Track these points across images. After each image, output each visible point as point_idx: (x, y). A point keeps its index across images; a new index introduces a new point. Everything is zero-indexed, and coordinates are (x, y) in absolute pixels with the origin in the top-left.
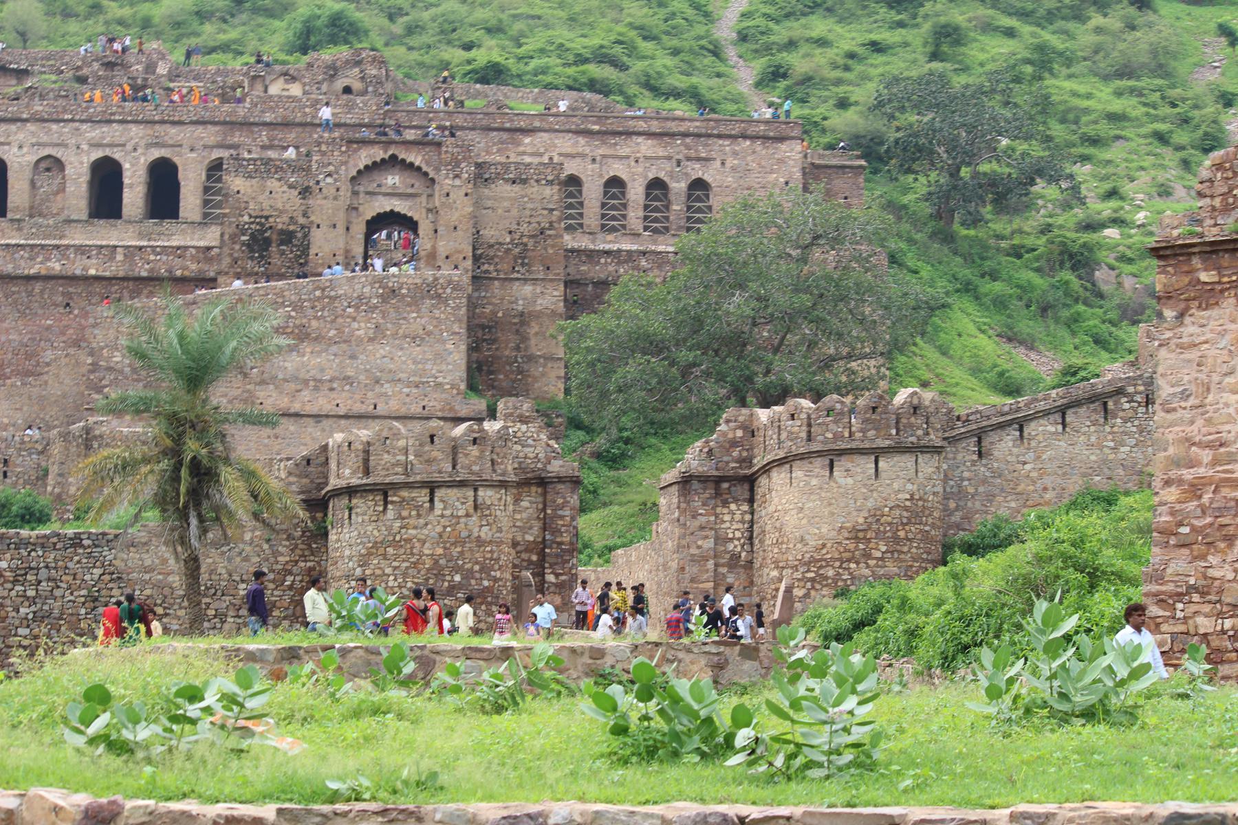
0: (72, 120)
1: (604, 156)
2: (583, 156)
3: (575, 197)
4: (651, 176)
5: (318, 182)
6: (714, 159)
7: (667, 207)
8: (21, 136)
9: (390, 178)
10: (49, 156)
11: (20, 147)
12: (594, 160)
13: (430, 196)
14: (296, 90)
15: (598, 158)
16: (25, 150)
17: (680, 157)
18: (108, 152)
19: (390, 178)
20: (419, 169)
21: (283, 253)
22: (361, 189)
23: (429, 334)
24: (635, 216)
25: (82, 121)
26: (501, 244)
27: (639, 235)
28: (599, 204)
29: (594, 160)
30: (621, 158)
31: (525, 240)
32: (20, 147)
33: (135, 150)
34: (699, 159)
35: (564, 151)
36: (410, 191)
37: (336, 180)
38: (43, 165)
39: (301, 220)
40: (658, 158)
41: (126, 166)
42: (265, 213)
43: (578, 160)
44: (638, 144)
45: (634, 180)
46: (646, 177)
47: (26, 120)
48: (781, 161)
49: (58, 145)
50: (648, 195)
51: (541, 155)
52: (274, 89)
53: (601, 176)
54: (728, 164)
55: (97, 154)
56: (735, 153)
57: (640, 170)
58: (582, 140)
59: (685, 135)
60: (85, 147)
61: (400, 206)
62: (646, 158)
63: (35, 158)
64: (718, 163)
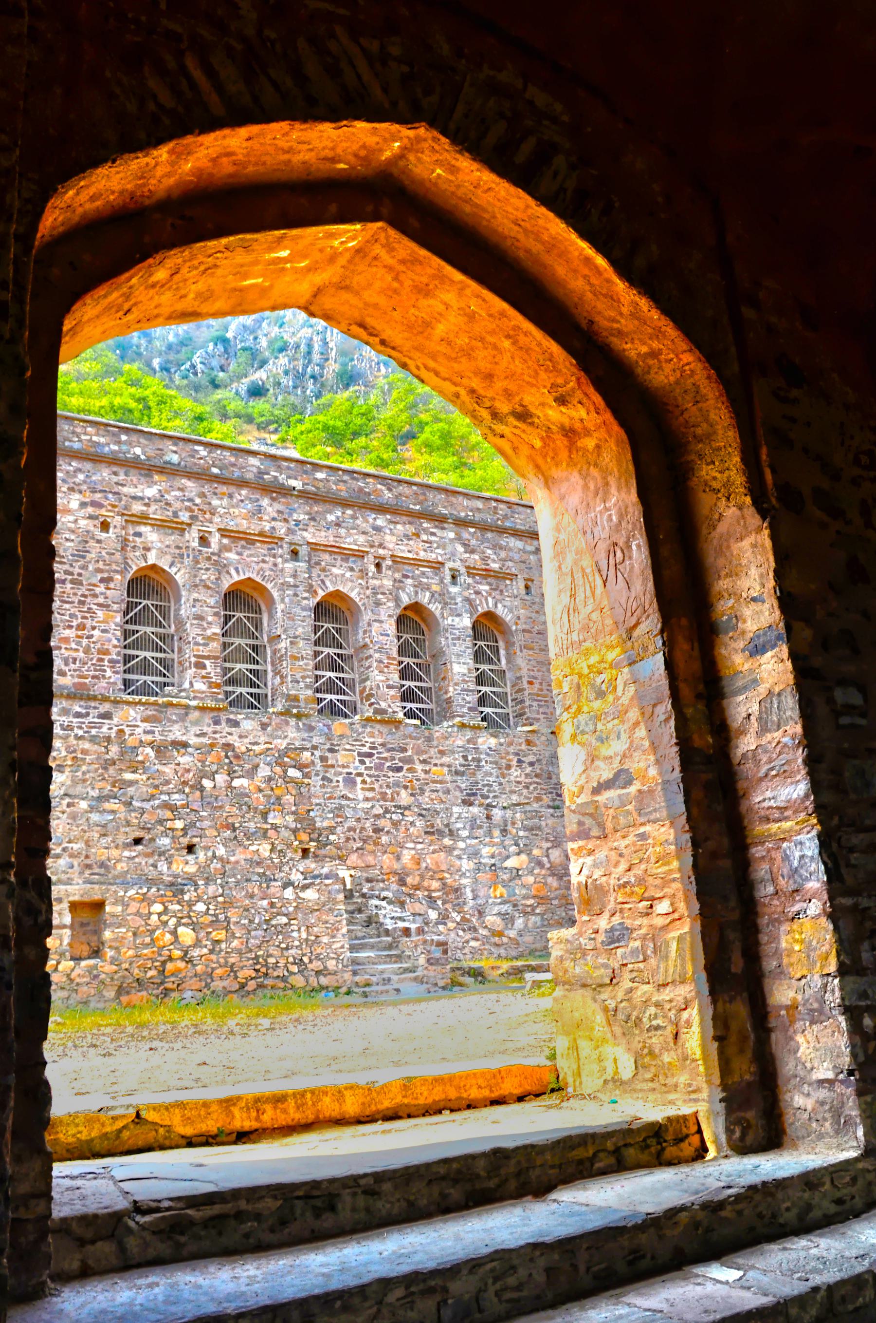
1: (314, 547)
2: (270, 539)
4: (406, 600)
6: (512, 577)
12: (295, 554)
15: (303, 551)
17: (457, 565)
24: (382, 679)
27: (398, 723)
28: (306, 649)
29: (295, 554)
34: (487, 574)
35: (232, 525)
40: (417, 563)
43: (261, 549)
44: (378, 529)
45: (378, 604)
51: (181, 529)
57: (388, 583)
59: (461, 523)
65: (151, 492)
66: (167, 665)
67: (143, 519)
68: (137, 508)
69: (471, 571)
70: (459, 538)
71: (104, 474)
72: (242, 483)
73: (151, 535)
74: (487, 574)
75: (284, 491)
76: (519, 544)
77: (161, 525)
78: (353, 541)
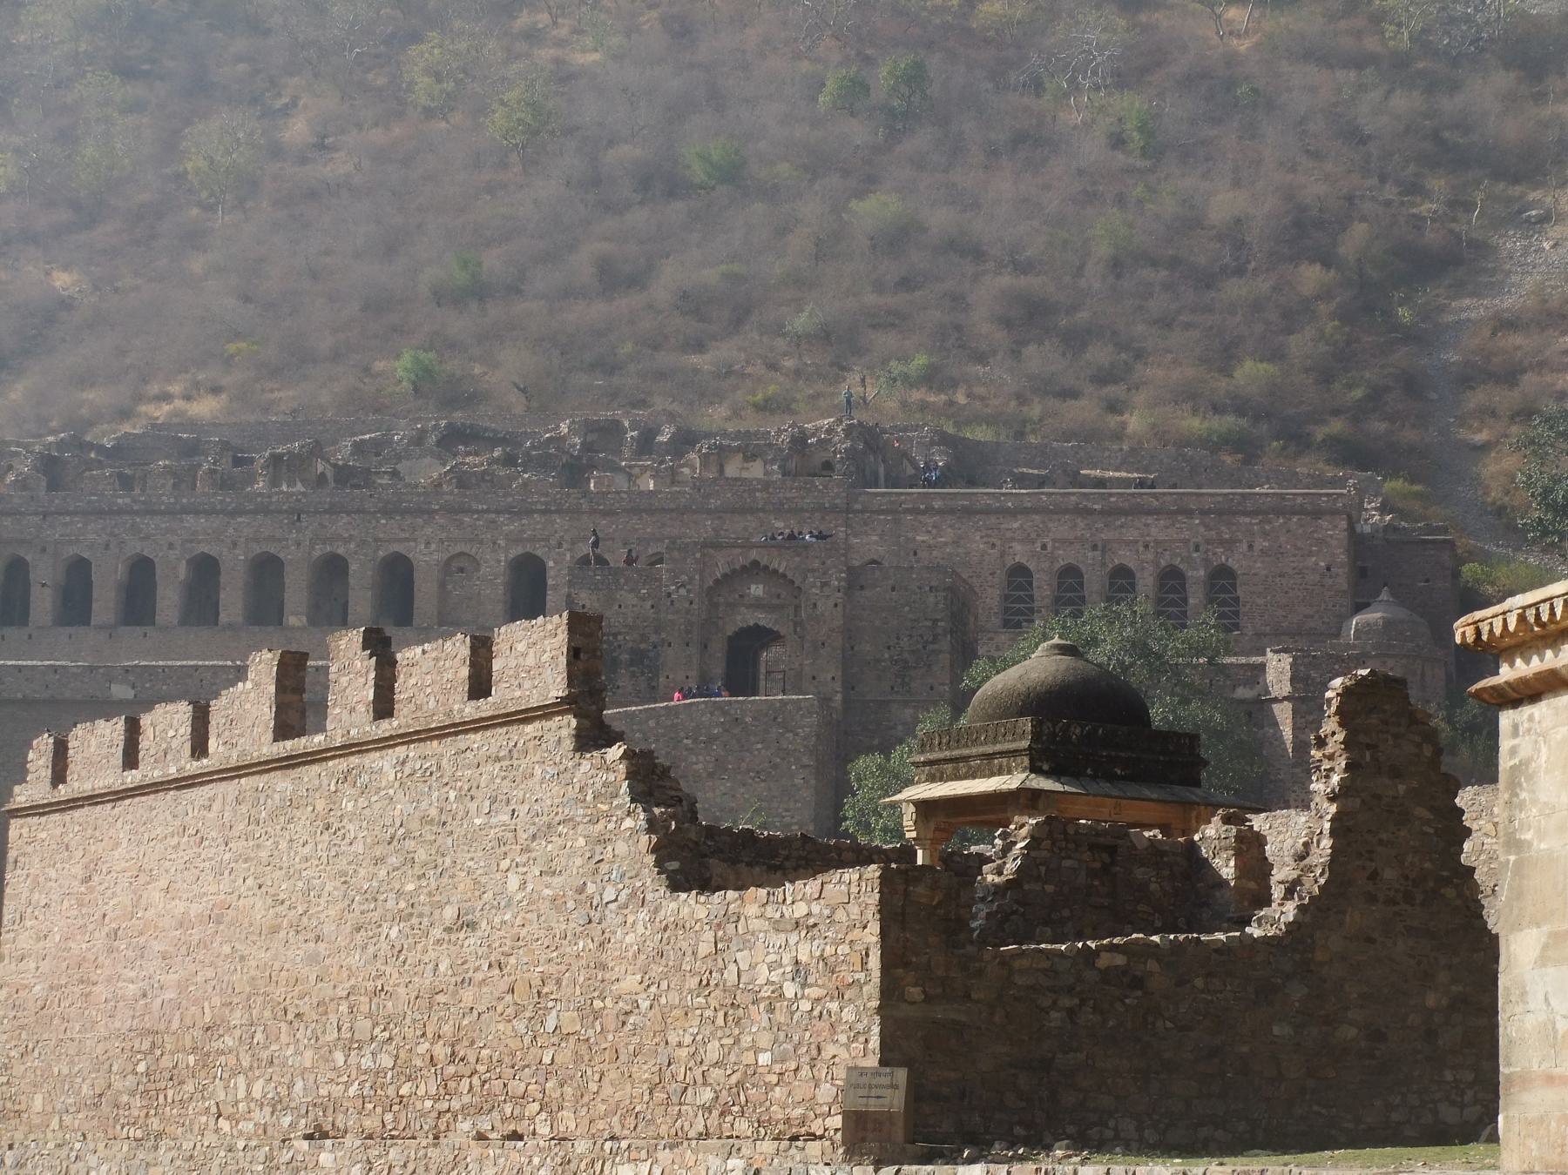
0: (487, 511)
3: (1075, 590)
4: (1163, 563)
5: (669, 595)
7: (1185, 600)
8: (428, 531)
9: (753, 587)
10: (461, 554)
11: (428, 544)
13: (797, 608)
14: (756, 470)
16: (433, 546)
18: (529, 549)
19: (753, 587)
20: (784, 576)
21: (633, 675)
22: (721, 600)
23: (775, 767)
25: (498, 512)
26: (878, 661)
30: (1128, 543)
31: (906, 655)
32: (428, 544)
33: (560, 545)
34: (1222, 542)
36: (775, 601)
37: (689, 591)
38: (455, 564)
39: (653, 638)
41: (551, 564)
42: (614, 630)
44: (1147, 525)
46: (1157, 565)
47: (435, 511)
48: (1321, 542)
49: (471, 540)
50: (1161, 586)
52: (731, 470)
53: (1104, 564)
54: (1257, 547)
55: (516, 551)
56: (1265, 534)
57: (1150, 556)
58: (1081, 523)
59: (1204, 513)
60: (502, 543)
61: (763, 619)
62: (1156, 541)
63: (445, 556)
64: (1245, 546)
65: (1016, 525)
66: (1032, 610)
67: (1013, 539)
68: (1009, 535)
69: (1208, 542)
70: (1202, 523)
71: (993, 520)
72: (1066, 511)
73: (1017, 547)
74: (1222, 542)
75: (1089, 512)
76: (1247, 520)
77: (1022, 541)
78: (1131, 534)
